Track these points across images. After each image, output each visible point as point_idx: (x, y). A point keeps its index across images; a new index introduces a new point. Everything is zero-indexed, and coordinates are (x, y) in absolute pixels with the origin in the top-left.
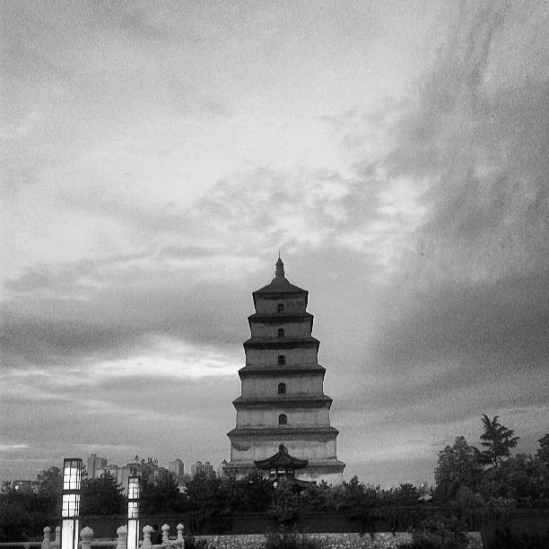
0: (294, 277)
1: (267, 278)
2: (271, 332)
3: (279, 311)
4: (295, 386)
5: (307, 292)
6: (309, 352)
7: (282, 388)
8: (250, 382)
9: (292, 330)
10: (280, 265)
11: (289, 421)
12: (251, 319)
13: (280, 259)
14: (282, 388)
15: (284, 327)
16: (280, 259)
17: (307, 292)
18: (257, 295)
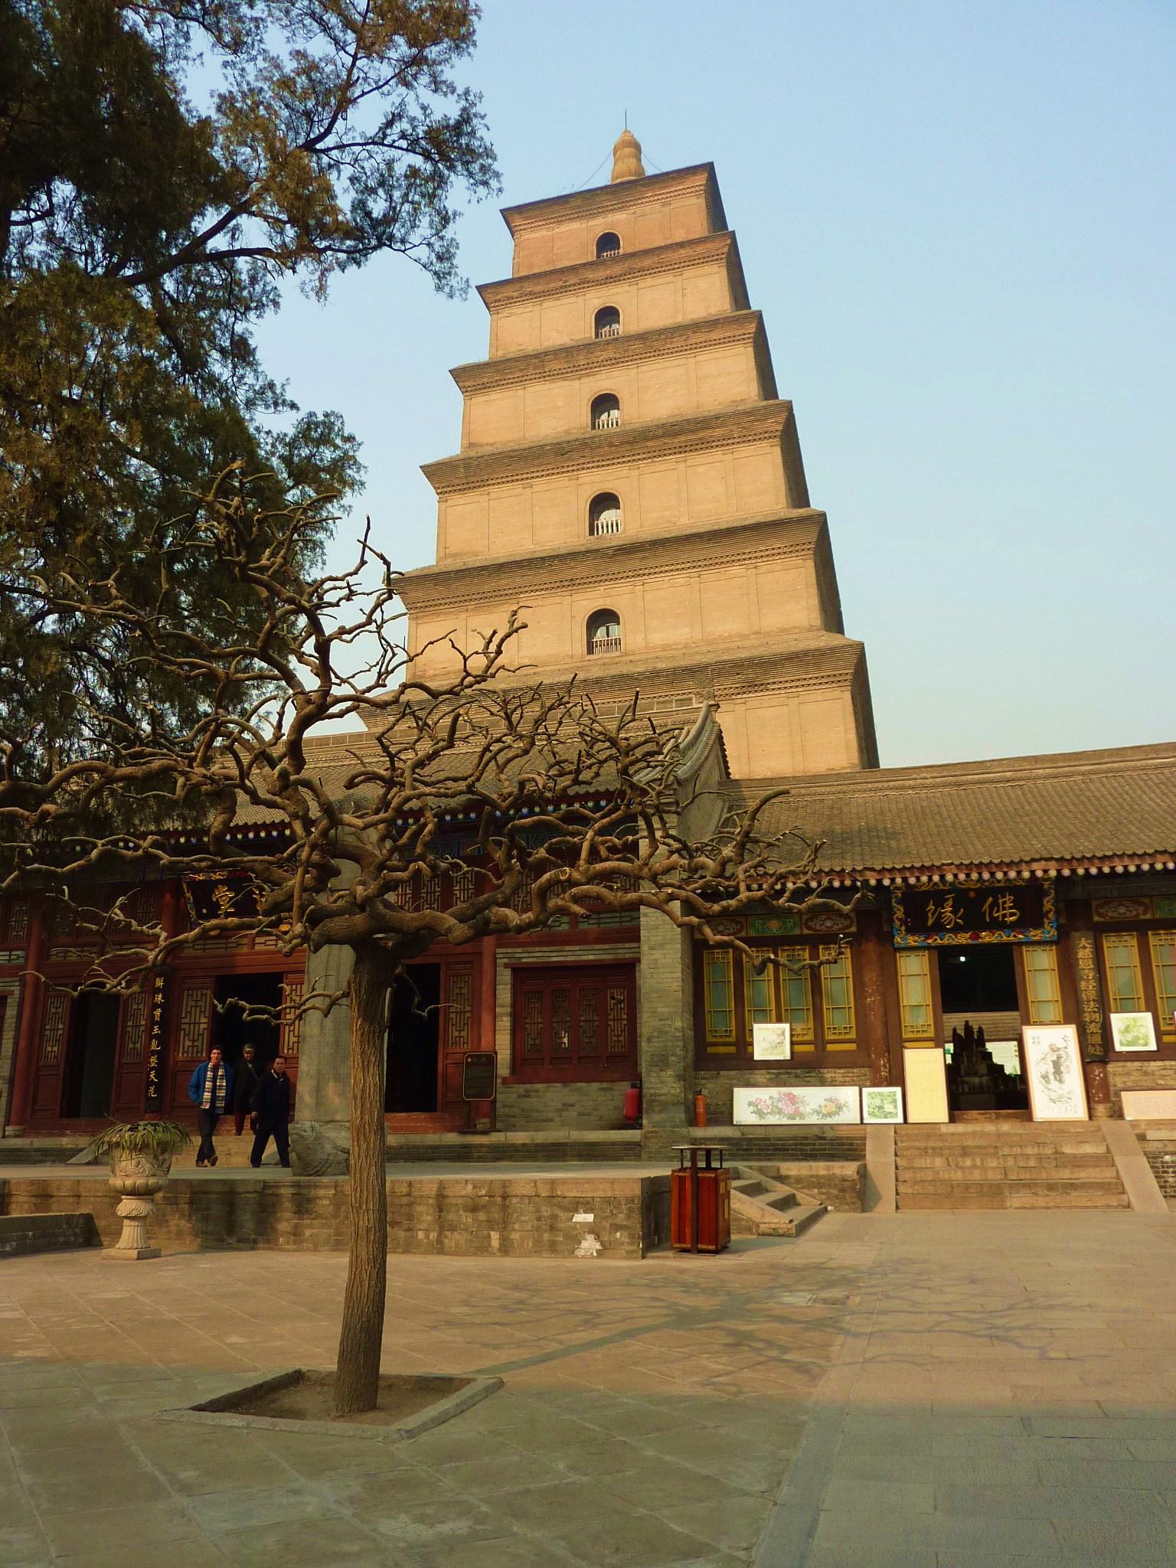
5: (709, 168)
15: (615, 295)
17: (709, 168)
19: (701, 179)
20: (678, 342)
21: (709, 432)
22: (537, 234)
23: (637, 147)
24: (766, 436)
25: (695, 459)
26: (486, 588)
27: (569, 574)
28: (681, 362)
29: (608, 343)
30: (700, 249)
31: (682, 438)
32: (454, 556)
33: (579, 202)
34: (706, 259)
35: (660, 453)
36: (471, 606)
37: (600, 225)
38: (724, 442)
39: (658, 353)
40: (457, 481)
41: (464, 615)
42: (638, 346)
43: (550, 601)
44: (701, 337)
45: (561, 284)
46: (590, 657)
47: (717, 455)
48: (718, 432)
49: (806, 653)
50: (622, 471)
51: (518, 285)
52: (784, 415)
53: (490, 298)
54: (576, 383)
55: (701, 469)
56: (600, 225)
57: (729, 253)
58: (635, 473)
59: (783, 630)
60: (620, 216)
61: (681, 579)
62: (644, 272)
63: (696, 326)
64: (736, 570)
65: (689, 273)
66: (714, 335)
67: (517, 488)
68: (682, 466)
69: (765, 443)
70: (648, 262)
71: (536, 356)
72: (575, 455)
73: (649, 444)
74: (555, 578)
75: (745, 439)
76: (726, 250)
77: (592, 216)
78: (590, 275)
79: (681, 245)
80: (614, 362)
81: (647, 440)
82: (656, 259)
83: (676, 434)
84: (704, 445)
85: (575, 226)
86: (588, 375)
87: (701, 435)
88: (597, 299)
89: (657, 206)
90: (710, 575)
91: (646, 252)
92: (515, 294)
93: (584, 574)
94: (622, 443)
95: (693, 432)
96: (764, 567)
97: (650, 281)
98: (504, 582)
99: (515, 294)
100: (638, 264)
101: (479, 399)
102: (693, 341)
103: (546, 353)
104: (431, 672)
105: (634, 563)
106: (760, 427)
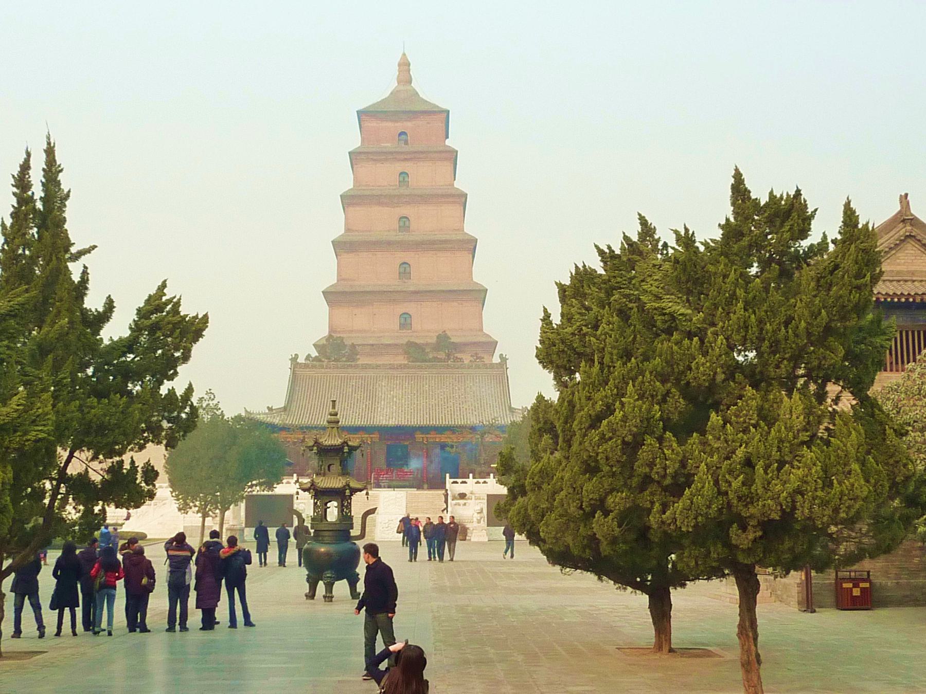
0: (429, 89)
1: (379, 88)
2: (384, 175)
4: (430, 270)
6: (448, 211)
7: (405, 270)
8: (349, 258)
9: (423, 175)
10: (405, 65)
11: (416, 325)
12: (355, 157)
13: (404, 54)
14: (405, 270)
15: (408, 167)
16: (404, 54)
18: (363, 115)
22: (372, 124)
23: (409, 65)
32: (343, 280)
34: (446, 159)
37: (400, 126)
56: (400, 126)
60: (409, 124)
63: (443, 196)
64: (455, 304)
66: (451, 200)
77: (396, 121)
80: (408, 203)
84: (446, 250)
85: (389, 124)
88: (399, 167)
91: (422, 152)
101: (351, 209)
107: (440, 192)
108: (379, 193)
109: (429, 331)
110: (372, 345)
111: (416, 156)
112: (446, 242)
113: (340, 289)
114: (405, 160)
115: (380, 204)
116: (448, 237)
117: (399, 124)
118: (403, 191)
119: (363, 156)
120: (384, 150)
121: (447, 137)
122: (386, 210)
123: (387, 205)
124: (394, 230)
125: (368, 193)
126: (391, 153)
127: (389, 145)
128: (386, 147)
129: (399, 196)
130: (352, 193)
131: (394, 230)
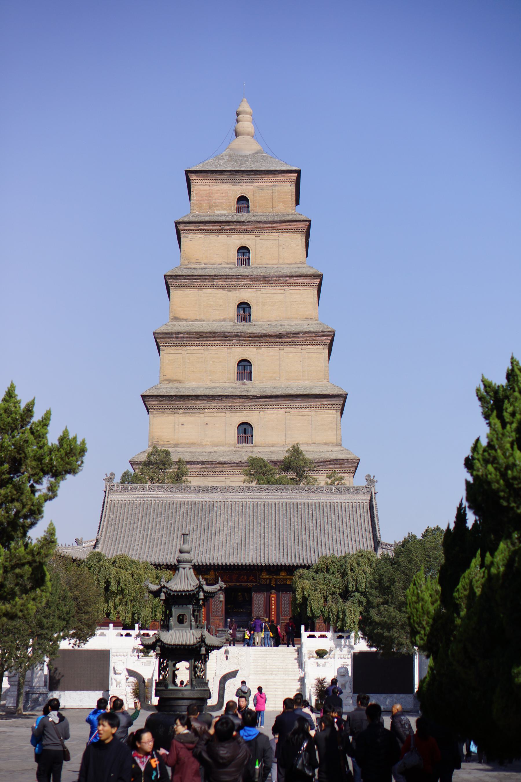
3: (239, 210)
17: (299, 172)
19: (294, 176)
20: (282, 281)
21: (296, 338)
24: (323, 344)
25: (288, 349)
26: (190, 404)
27: (230, 403)
28: (282, 291)
29: (247, 276)
30: (293, 225)
31: (284, 339)
32: (170, 381)
33: (228, 175)
34: (296, 230)
35: (273, 344)
36: (181, 412)
38: (302, 344)
39: (270, 285)
40: (171, 341)
41: (177, 416)
42: (262, 280)
43: (220, 414)
44: (292, 281)
45: (220, 228)
46: (240, 445)
47: (298, 349)
48: (301, 339)
49: (337, 461)
50: (253, 349)
51: (197, 225)
52: (330, 337)
53: (181, 227)
54: (229, 293)
55: (291, 355)
57: (307, 229)
58: (259, 351)
59: (326, 444)
61: (281, 412)
62: (263, 231)
63: (291, 277)
64: (307, 412)
65: (286, 236)
66: (299, 281)
67: (201, 349)
68: (282, 352)
69: (321, 347)
70: (266, 226)
71: (210, 276)
72: (231, 339)
73: (268, 339)
74: (224, 404)
75: (312, 344)
76: (306, 228)
77: (235, 183)
78: (238, 227)
79: (284, 222)
80: (249, 286)
81: (267, 337)
82: (270, 226)
83: (281, 337)
84: (293, 344)
85: (225, 187)
86: (235, 290)
87: (293, 339)
88: (238, 240)
89: (270, 185)
90: (295, 412)
91: (266, 222)
92: (196, 229)
93: (237, 404)
94: (255, 337)
95: (289, 337)
96: (319, 411)
97: (265, 236)
98: (198, 403)
99: (196, 229)
100: (261, 226)
102: (289, 282)
103: (215, 276)
104: (161, 443)
105: (260, 403)
106: (320, 339)
107: (288, 272)
108: (213, 273)
109: (274, 445)
110: (203, 462)
111: (259, 226)
112: (295, 335)
113: (163, 392)
114: (245, 231)
115: (212, 286)
116: (299, 329)
117: (238, 187)
118: (243, 270)
119: (192, 227)
120: (220, 219)
121: (297, 203)
122: (221, 294)
123: (221, 287)
124: (231, 320)
125: (200, 273)
126: (228, 223)
127: (225, 212)
128: (219, 216)
129: (238, 277)
130: (180, 273)
131: (231, 320)
